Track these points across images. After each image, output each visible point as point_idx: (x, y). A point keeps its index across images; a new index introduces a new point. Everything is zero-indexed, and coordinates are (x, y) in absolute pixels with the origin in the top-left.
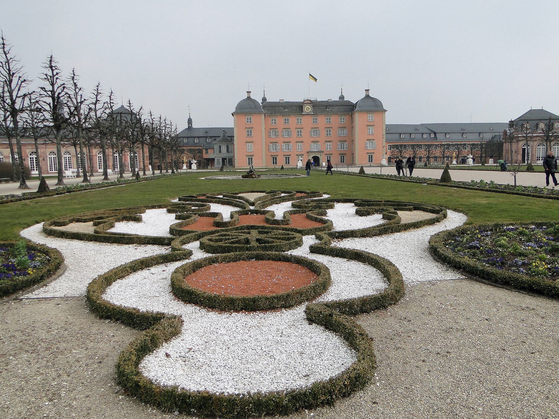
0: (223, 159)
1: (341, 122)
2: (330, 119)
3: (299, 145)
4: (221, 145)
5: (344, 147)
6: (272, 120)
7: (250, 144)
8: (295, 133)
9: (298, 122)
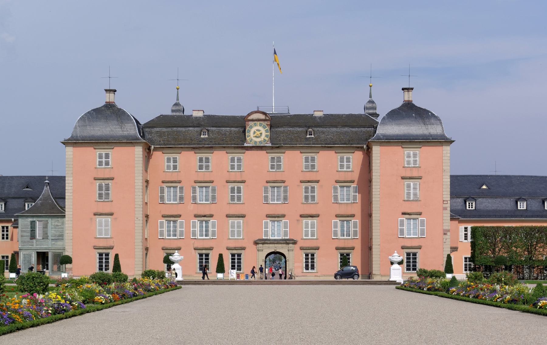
1: (342, 166)
2: (313, 159)
3: (233, 223)
4: (34, 219)
6: (169, 160)
7: (103, 219)
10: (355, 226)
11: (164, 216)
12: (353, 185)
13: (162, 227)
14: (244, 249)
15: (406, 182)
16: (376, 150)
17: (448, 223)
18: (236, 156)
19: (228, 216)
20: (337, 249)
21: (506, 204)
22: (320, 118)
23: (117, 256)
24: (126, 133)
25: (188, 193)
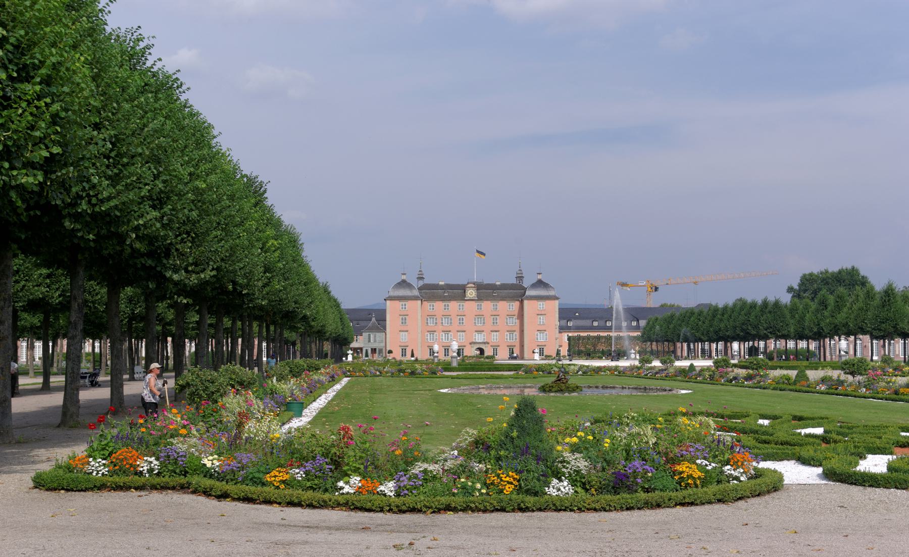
0: (372, 349)
1: (510, 308)
2: (496, 305)
5: (513, 338)
7: (404, 333)
8: (456, 320)
9: (460, 309)
10: (516, 336)
11: (428, 331)
12: (516, 317)
13: (427, 336)
14: (465, 346)
15: (539, 316)
16: (526, 302)
17: (558, 335)
18: (461, 304)
19: (458, 331)
21: (587, 323)
22: (499, 285)
25: (439, 321)
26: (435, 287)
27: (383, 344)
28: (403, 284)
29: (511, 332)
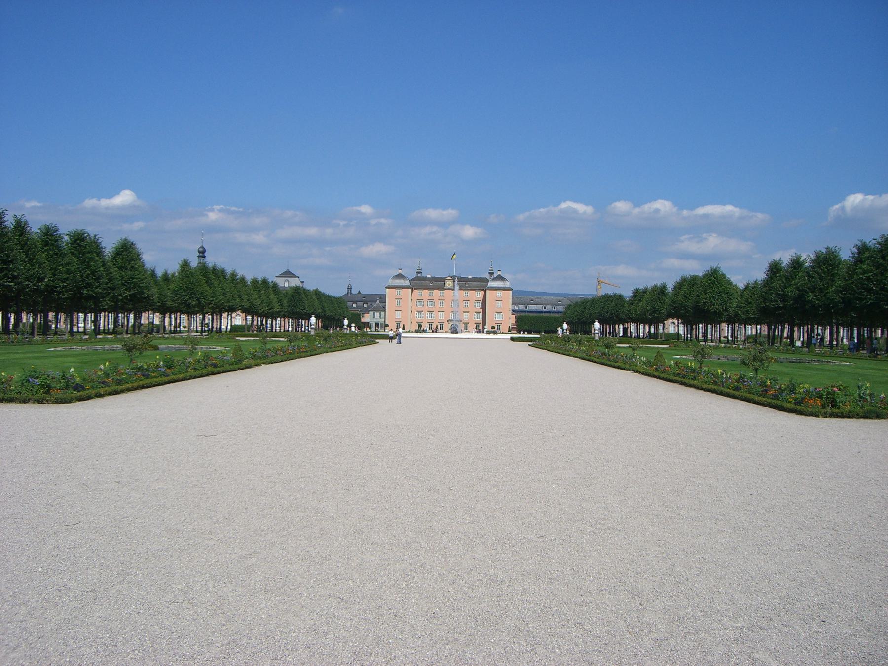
0: (376, 323)
2: (468, 293)
12: (481, 302)
14: (444, 323)
16: (487, 291)
18: (442, 292)
20: (475, 323)
23: (404, 325)
24: (406, 284)
25: (425, 304)
26: (425, 279)
27: (383, 320)
28: (400, 276)
29: (478, 313)
